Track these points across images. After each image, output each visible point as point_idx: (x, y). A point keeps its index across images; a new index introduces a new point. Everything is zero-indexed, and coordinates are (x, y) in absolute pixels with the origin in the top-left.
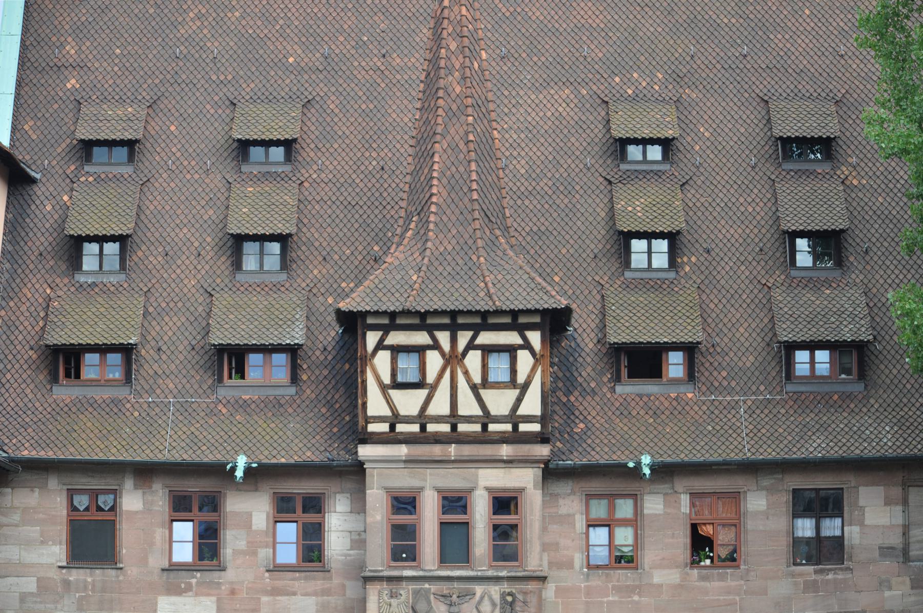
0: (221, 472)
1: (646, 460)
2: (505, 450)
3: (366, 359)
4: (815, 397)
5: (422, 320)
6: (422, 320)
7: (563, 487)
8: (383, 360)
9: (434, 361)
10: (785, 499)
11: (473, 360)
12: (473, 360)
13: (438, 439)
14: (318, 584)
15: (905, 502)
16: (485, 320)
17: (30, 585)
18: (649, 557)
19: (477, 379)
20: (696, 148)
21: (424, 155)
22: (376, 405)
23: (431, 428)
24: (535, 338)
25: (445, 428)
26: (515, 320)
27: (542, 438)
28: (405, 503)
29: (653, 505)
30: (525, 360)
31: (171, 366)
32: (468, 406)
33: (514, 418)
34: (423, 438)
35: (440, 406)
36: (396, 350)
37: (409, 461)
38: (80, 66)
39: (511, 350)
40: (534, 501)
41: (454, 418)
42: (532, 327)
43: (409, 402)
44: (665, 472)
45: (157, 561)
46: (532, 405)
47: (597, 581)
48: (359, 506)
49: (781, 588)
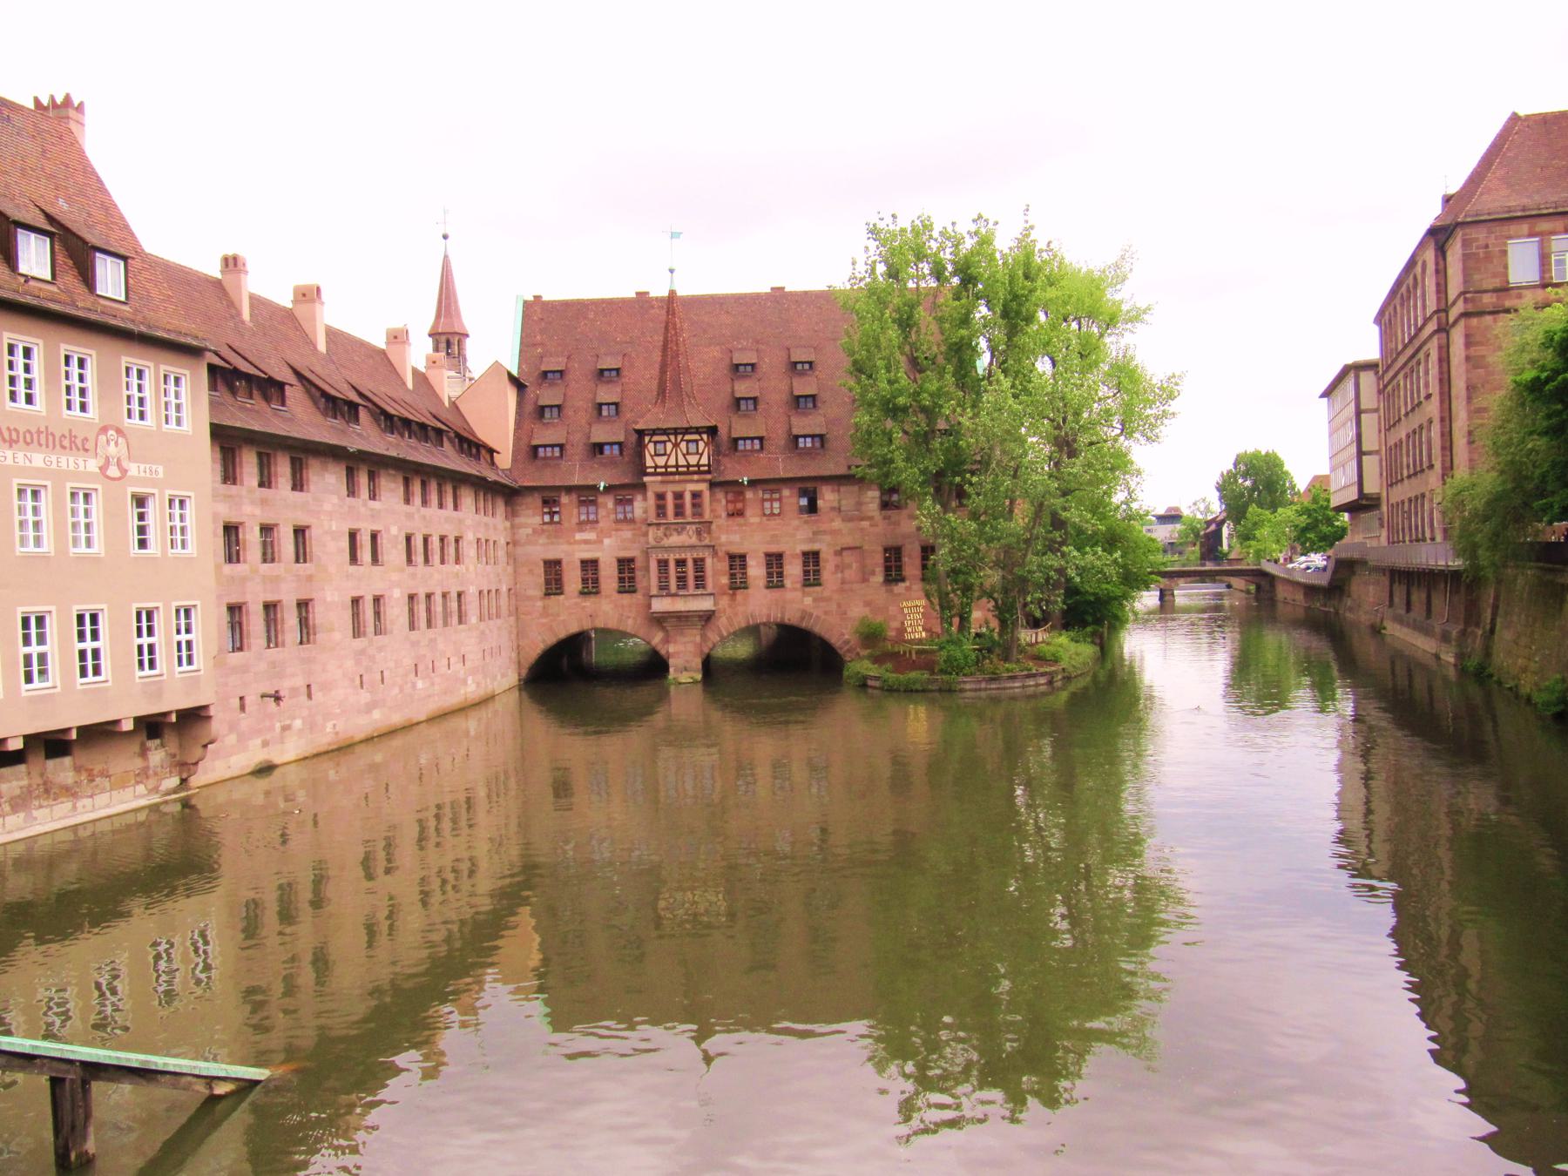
0: (595, 488)
2: (696, 477)
4: (807, 452)
5: (665, 432)
6: (665, 432)
7: (717, 490)
8: (651, 446)
9: (669, 446)
10: (796, 491)
11: (683, 445)
12: (683, 445)
16: (687, 431)
17: (530, 531)
18: (748, 513)
20: (764, 367)
22: (649, 462)
24: (705, 437)
26: (698, 431)
27: (709, 472)
28: (661, 497)
29: (749, 495)
30: (701, 444)
31: (577, 451)
32: (682, 462)
33: (698, 465)
34: (666, 474)
35: (672, 462)
36: (656, 443)
37: (662, 482)
38: (542, 344)
39: (696, 441)
40: (706, 495)
41: (677, 466)
43: (661, 461)
44: (753, 483)
45: (575, 520)
46: (704, 461)
48: (645, 499)
49: (796, 523)
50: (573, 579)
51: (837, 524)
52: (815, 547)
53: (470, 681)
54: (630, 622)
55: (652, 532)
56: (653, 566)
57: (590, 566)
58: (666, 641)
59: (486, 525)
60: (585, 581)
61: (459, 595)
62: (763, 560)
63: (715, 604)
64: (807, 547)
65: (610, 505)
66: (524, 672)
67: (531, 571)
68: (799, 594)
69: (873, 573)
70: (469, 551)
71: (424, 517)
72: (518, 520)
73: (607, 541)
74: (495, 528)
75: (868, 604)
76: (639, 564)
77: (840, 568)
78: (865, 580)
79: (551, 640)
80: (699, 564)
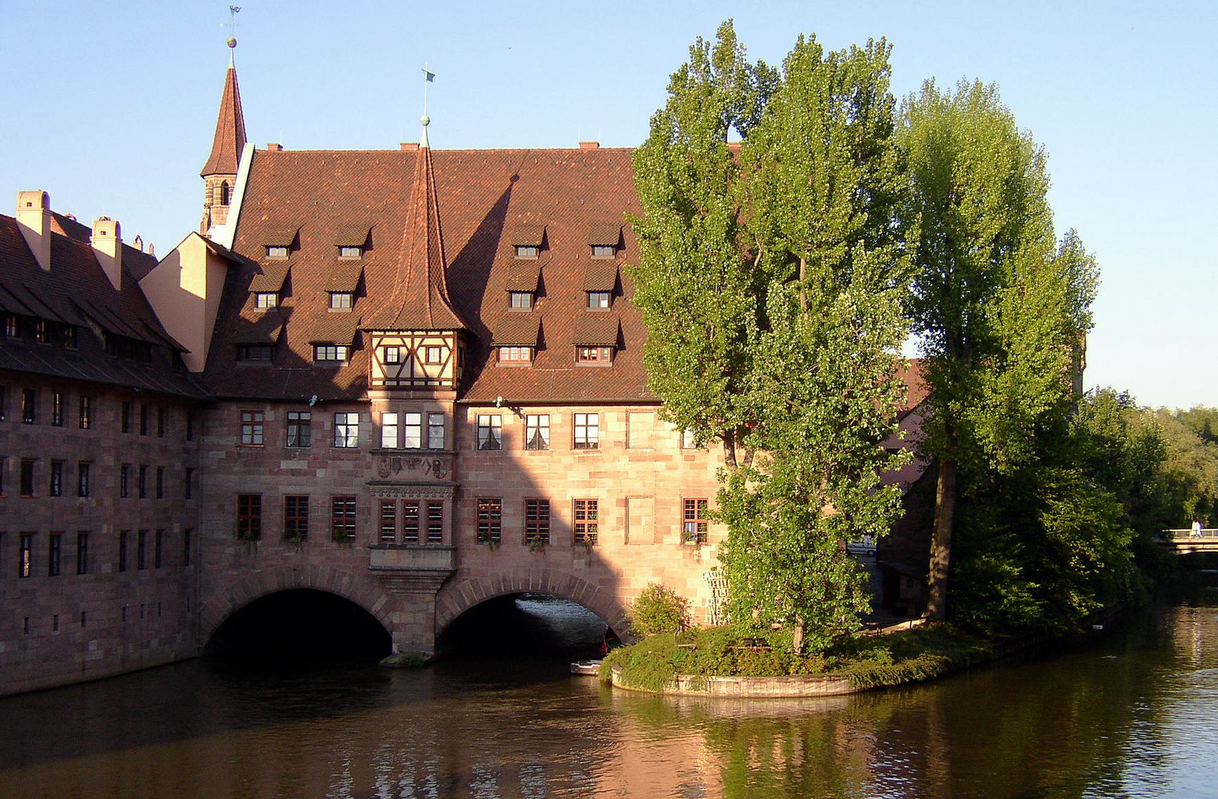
1: (500, 399)
3: (373, 351)
13: (405, 388)
14: (354, 456)
15: (627, 420)
17: (222, 454)
19: (423, 361)
21: (406, 255)
23: (401, 383)
24: (450, 342)
25: (409, 383)
30: (445, 350)
39: (439, 347)
42: (449, 336)
46: (449, 373)
47: (482, 455)
49: (568, 460)
50: (273, 520)
51: (623, 464)
52: (592, 494)
53: (91, 647)
54: (345, 580)
55: (376, 462)
56: (375, 507)
57: (297, 506)
58: (391, 607)
59: (142, 445)
60: (290, 524)
61: (83, 536)
62: (521, 508)
63: (456, 559)
64: (580, 494)
65: (328, 426)
66: (205, 639)
67: (221, 508)
68: (569, 555)
69: (668, 532)
70: (106, 480)
71: (26, 437)
72: (208, 440)
73: (320, 473)
74: (164, 450)
75: (659, 572)
76: (359, 504)
77: (626, 522)
78: (658, 540)
79: (242, 599)
80: (434, 508)
